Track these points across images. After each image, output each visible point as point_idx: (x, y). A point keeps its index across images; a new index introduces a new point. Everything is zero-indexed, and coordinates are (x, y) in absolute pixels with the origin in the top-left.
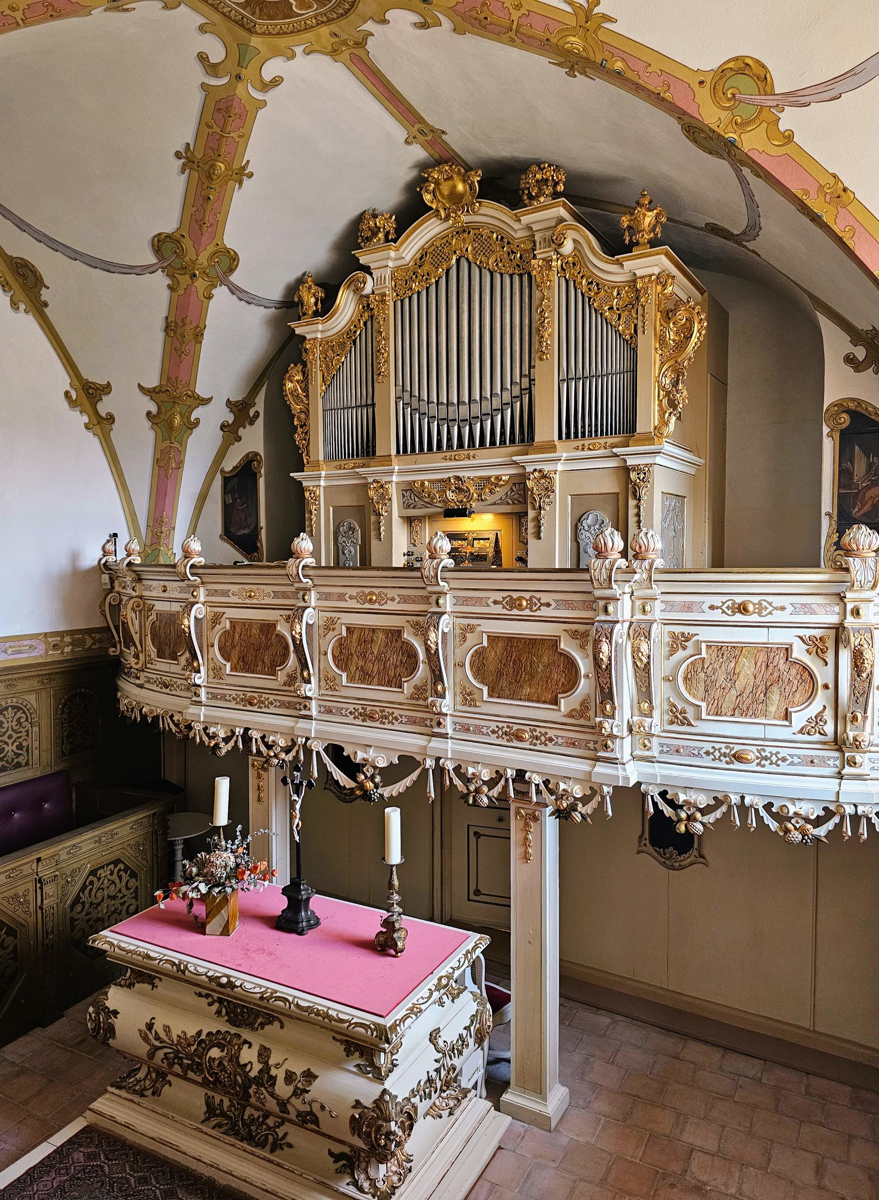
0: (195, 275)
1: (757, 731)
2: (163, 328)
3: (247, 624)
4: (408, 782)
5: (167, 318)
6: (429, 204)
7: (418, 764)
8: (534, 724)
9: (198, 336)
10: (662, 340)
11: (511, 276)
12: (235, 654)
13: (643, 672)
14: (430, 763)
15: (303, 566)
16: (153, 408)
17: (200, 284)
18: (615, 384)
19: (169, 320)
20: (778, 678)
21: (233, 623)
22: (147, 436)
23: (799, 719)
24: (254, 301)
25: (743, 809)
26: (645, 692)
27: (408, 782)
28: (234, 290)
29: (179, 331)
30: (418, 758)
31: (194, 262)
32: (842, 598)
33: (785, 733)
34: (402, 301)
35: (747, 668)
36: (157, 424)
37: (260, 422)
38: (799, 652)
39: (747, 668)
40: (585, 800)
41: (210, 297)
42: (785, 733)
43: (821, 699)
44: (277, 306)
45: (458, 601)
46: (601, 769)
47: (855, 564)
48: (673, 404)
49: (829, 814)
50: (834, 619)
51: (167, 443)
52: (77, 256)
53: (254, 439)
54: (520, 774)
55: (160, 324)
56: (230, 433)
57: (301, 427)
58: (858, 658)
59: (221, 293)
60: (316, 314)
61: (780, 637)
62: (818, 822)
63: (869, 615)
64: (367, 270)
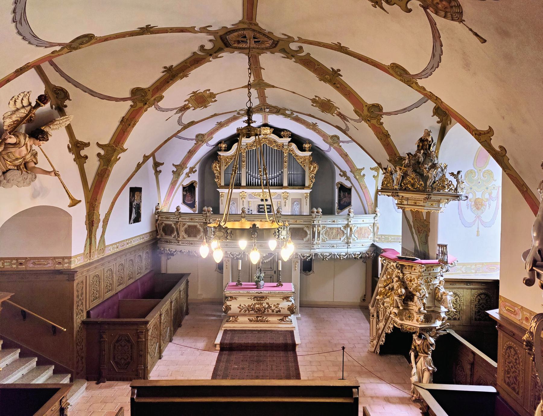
1: (336, 242)
10: (310, 168)
13: (319, 233)
16: (175, 170)
18: (300, 176)
20: (340, 232)
22: (170, 177)
23: (342, 239)
25: (334, 255)
26: (319, 236)
33: (340, 242)
35: (334, 231)
37: (197, 173)
38: (342, 229)
39: (334, 231)
40: (309, 257)
42: (340, 242)
43: (345, 235)
46: (312, 250)
47: (350, 214)
48: (312, 181)
49: (346, 254)
53: (195, 177)
56: (188, 175)
58: (351, 229)
62: (345, 256)
63: (352, 222)
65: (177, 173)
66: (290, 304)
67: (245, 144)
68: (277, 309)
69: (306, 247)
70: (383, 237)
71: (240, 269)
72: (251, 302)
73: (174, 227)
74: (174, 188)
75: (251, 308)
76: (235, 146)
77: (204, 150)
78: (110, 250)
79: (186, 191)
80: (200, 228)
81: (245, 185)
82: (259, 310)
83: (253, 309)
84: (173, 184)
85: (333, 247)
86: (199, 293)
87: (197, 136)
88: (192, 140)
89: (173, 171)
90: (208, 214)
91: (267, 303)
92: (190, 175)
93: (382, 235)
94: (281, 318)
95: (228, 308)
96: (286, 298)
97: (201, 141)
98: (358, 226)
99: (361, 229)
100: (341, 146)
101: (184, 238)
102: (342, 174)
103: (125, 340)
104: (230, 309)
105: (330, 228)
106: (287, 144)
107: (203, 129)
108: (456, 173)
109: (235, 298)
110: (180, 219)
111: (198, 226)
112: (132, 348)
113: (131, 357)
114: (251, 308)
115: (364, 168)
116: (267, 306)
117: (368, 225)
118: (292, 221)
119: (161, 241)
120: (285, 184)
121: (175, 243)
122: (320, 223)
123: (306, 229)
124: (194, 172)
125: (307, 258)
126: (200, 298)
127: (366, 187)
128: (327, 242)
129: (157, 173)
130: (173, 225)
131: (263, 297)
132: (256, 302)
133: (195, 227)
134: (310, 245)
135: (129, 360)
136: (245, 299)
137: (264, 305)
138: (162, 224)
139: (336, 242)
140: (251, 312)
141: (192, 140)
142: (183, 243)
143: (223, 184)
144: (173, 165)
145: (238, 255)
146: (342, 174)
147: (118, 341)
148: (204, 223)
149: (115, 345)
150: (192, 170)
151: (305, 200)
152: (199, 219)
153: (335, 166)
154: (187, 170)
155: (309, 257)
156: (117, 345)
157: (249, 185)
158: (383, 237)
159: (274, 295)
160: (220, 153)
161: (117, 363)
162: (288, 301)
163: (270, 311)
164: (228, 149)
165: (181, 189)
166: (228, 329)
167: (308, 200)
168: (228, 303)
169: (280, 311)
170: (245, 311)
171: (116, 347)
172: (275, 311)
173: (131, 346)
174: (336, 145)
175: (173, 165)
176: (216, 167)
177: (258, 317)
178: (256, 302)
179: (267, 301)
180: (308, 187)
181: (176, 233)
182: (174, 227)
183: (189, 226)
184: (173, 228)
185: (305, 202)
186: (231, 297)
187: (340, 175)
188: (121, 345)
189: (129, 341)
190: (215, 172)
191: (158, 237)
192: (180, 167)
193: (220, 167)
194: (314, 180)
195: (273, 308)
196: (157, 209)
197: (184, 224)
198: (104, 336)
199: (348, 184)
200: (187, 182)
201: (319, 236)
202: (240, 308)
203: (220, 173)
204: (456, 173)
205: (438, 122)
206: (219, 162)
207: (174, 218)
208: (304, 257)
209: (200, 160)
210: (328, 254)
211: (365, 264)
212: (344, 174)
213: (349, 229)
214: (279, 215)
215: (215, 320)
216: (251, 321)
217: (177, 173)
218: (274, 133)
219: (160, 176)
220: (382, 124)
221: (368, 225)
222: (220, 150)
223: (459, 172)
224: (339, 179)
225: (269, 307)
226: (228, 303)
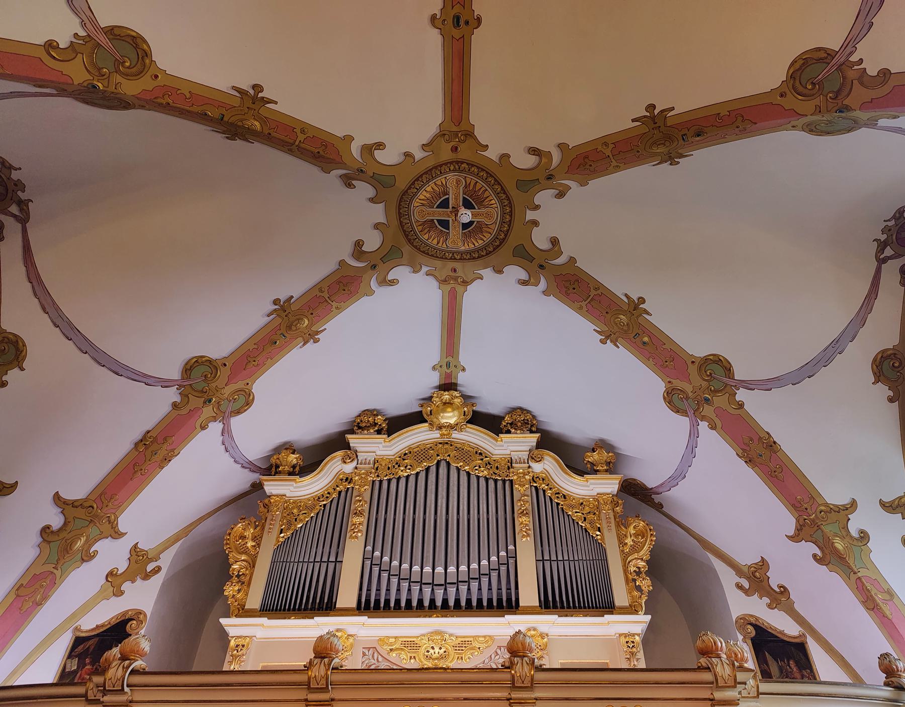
0: (210, 401)
2: (136, 441)
5: (148, 432)
6: (425, 416)
9: (167, 460)
11: (487, 480)
15: (333, 669)
19: (149, 435)
24: (231, 451)
28: (226, 431)
29: (154, 447)
34: (381, 482)
36: (49, 542)
41: (203, 428)
44: (246, 465)
51: (50, 567)
52: (88, 349)
55: (137, 435)
57: (238, 576)
59: (216, 427)
67: (371, 457)
76: (335, 467)
81: (354, 605)
100: (741, 405)
102: (746, 585)
106: (525, 455)
115: (853, 505)
120: (529, 595)
141: (166, 384)
146: (746, 585)
160: (273, 487)
174: (720, 401)
180: (631, 610)
187: (739, 587)
194: (646, 584)
199: (782, 624)
206: (261, 524)
212: (756, 579)
224: (741, 605)
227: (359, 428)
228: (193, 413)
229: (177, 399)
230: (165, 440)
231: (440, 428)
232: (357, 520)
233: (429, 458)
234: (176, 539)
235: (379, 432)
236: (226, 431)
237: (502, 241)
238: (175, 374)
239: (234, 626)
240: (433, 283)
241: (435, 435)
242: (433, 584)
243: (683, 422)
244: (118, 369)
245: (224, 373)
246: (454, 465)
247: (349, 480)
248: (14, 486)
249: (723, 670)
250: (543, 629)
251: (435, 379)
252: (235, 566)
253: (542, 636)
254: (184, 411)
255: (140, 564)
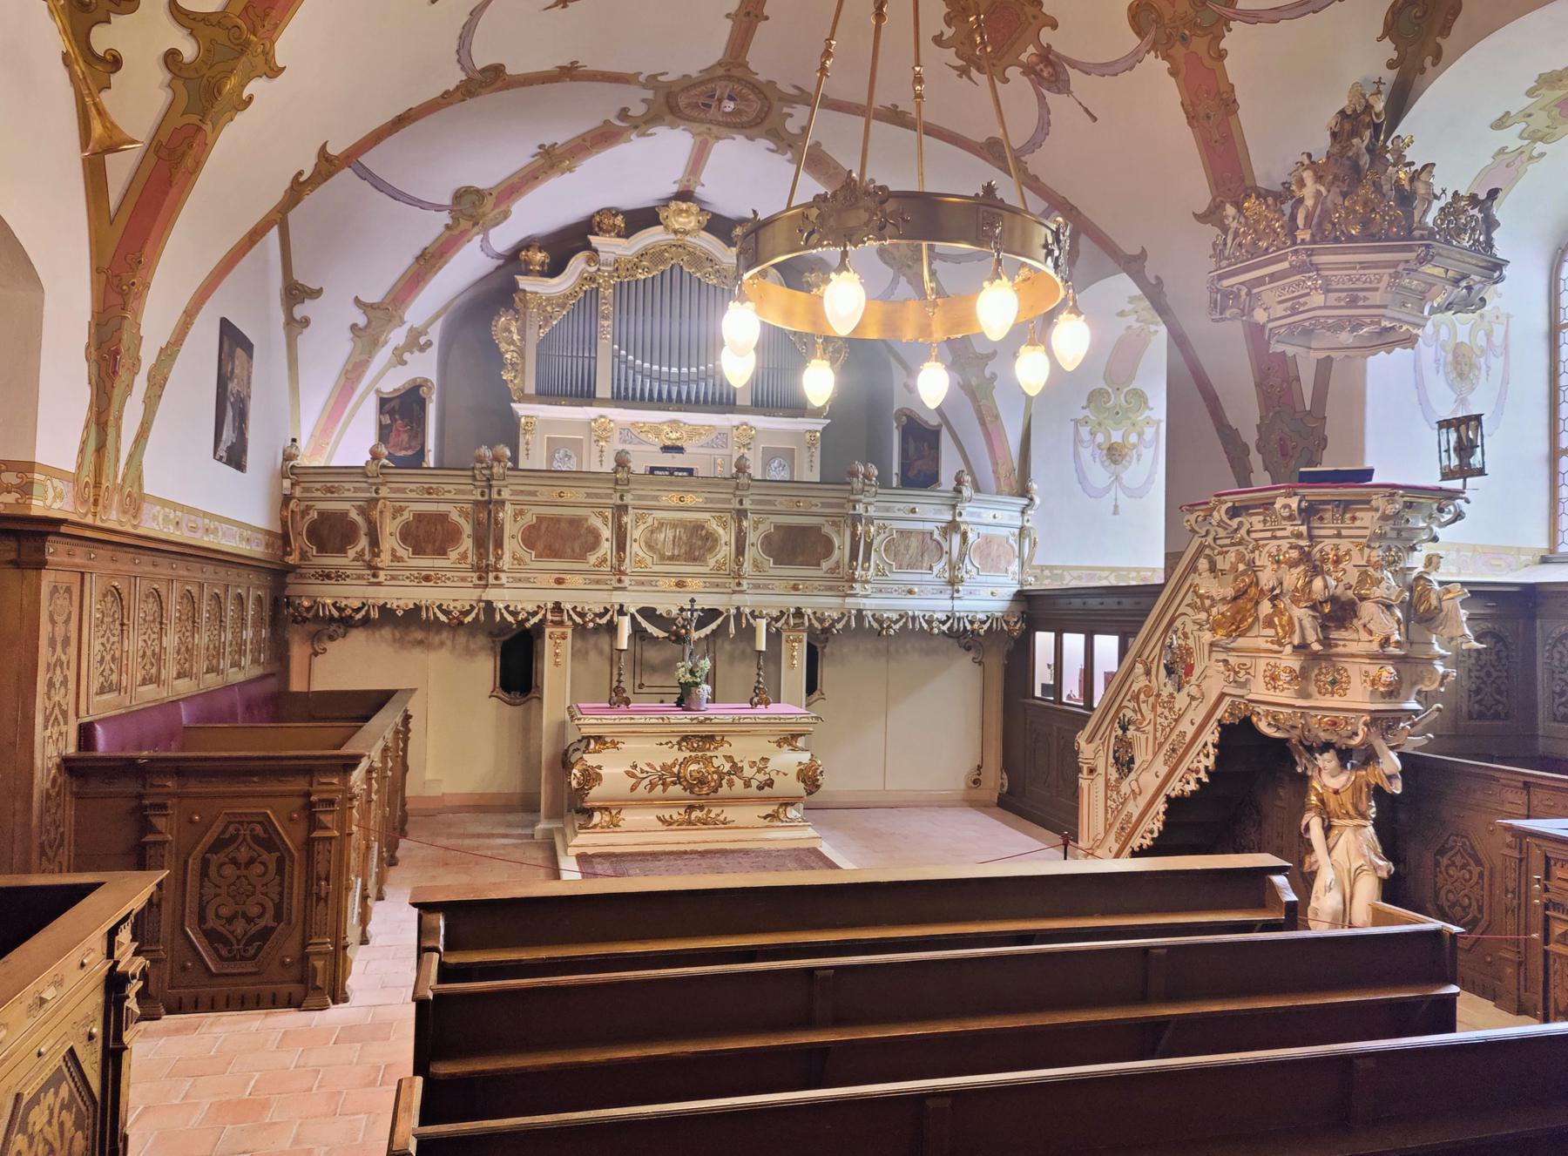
3: (556, 520)
4: (714, 626)
7: (721, 613)
8: (806, 579)
12: (540, 545)
14: (733, 611)
17: (476, 229)
21: (540, 519)
22: (342, 348)
27: (714, 626)
30: (721, 609)
31: (484, 214)
32: (954, 507)
35: (914, 542)
39: (914, 542)
45: (754, 502)
46: (848, 600)
50: (950, 518)
51: (364, 357)
53: (424, 367)
54: (798, 610)
55: (417, 251)
58: (964, 536)
59: (477, 239)
60: (543, 274)
61: (929, 526)
63: (965, 518)
64: (596, 251)
65: (367, 337)
66: (805, 757)
67: (611, 258)
68: (762, 777)
69: (830, 588)
70: (1047, 573)
71: (625, 647)
72: (673, 755)
73: (359, 519)
74: (353, 390)
75: (673, 775)
76: (577, 265)
77: (469, 265)
78: (155, 518)
79: (391, 413)
80: (462, 521)
82: (702, 781)
83: (679, 779)
84: (352, 373)
85: (910, 592)
86: (429, 775)
87: (459, 195)
88: (439, 208)
89: (354, 327)
90: (497, 470)
91: (729, 758)
92: (407, 356)
93: (1042, 568)
94: (769, 810)
95: (591, 777)
96: (789, 739)
97: (471, 217)
98: (983, 530)
99: (988, 540)
101: (395, 558)
103: (255, 838)
104: (599, 778)
105: (901, 532)
107: (487, 166)
108: (1482, 196)
109: (615, 744)
110: (384, 492)
111: (455, 516)
112: (280, 870)
113: (278, 908)
114: (673, 775)
116: (727, 767)
117: (1005, 532)
118: (781, 504)
119: (302, 576)
121: (359, 577)
122: (872, 512)
123: (827, 530)
124: (422, 349)
125: (832, 625)
126: (436, 791)
127: (997, 417)
128: (892, 577)
129: (295, 325)
130: (354, 515)
131: (710, 738)
132: (687, 754)
133: (443, 518)
134: (844, 582)
135: (268, 920)
136: (650, 745)
137: (716, 763)
138: (305, 513)
139: (918, 577)
140: (671, 788)
141: (439, 208)
142: (393, 578)
143: (531, 388)
144: (357, 300)
145: (601, 615)
147: (218, 845)
148: (476, 503)
149: (205, 863)
150: (415, 342)
151: (806, 455)
152: (458, 492)
153: (892, 360)
154: (397, 337)
155: (839, 620)
156: (214, 857)
157: (622, 398)
158: (1047, 573)
159: (745, 729)
160: (525, 283)
161: (212, 937)
162: (795, 749)
163: (739, 783)
164: (555, 268)
165: (371, 404)
166: (590, 851)
167: (817, 453)
168: (591, 760)
169: (770, 783)
170: (652, 786)
171: (213, 871)
172: (754, 783)
173: (280, 862)
175: (357, 300)
176: (507, 330)
177: (691, 808)
178: (687, 754)
179: (725, 750)
181: (363, 542)
182: (359, 519)
183: (419, 517)
184: (353, 524)
185: (806, 460)
186: (598, 739)
188: (234, 861)
189: (269, 842)
190: (503, 347)
191: (293, 559)
192: (379, 313)
193: (522, 332)
195: (748, 772)
196: (288, 457)
197: (401, 510)
198: (160, 823)
200: (394, 382)
201: (867, 558)
202: (633, 776)
203: (521, 353)
204: (1482, 196)
205: (1391, 65)
207: (356, 490)
208: (821, 620)
209: (445, 308)
210: (895, 616)
211: (978, 669)
213: (956, 539)
214: (743, 480)
215: (515, 846)
216: (668, 823)
217: (367, 337)
218: (709, 228)
219: (305, 339)
220: (1222, 55)
221: (1005, 532)
222: (528, 273)
223: (1493, 194)
225: (736, 769)
226: (591, 760)
227: (601, 229)
228: (463, 233)
229: (449, 221)
230: (441, 256)
231: (676, 232)
232: (606, 323)
233: (664, 262)
234: (436, 317)
235: (619, 236)
236: (486, 239)
237: (763, 120)
238: (447, 201)
239: (522, 409)
240: (688, 135)
241: (672, 236)
242: (669, 382)
243: (889, 272)
244: (396, 195)
245: (490, 202)
246: (686, 269)
247: (592, 279)
248: (319, 292)
249: (858, 485)
250: (753, 424)
251: (675, 189)
252: (508, 356)
253: (751, 428)
254: (456, 232)
255: (415, 342)
